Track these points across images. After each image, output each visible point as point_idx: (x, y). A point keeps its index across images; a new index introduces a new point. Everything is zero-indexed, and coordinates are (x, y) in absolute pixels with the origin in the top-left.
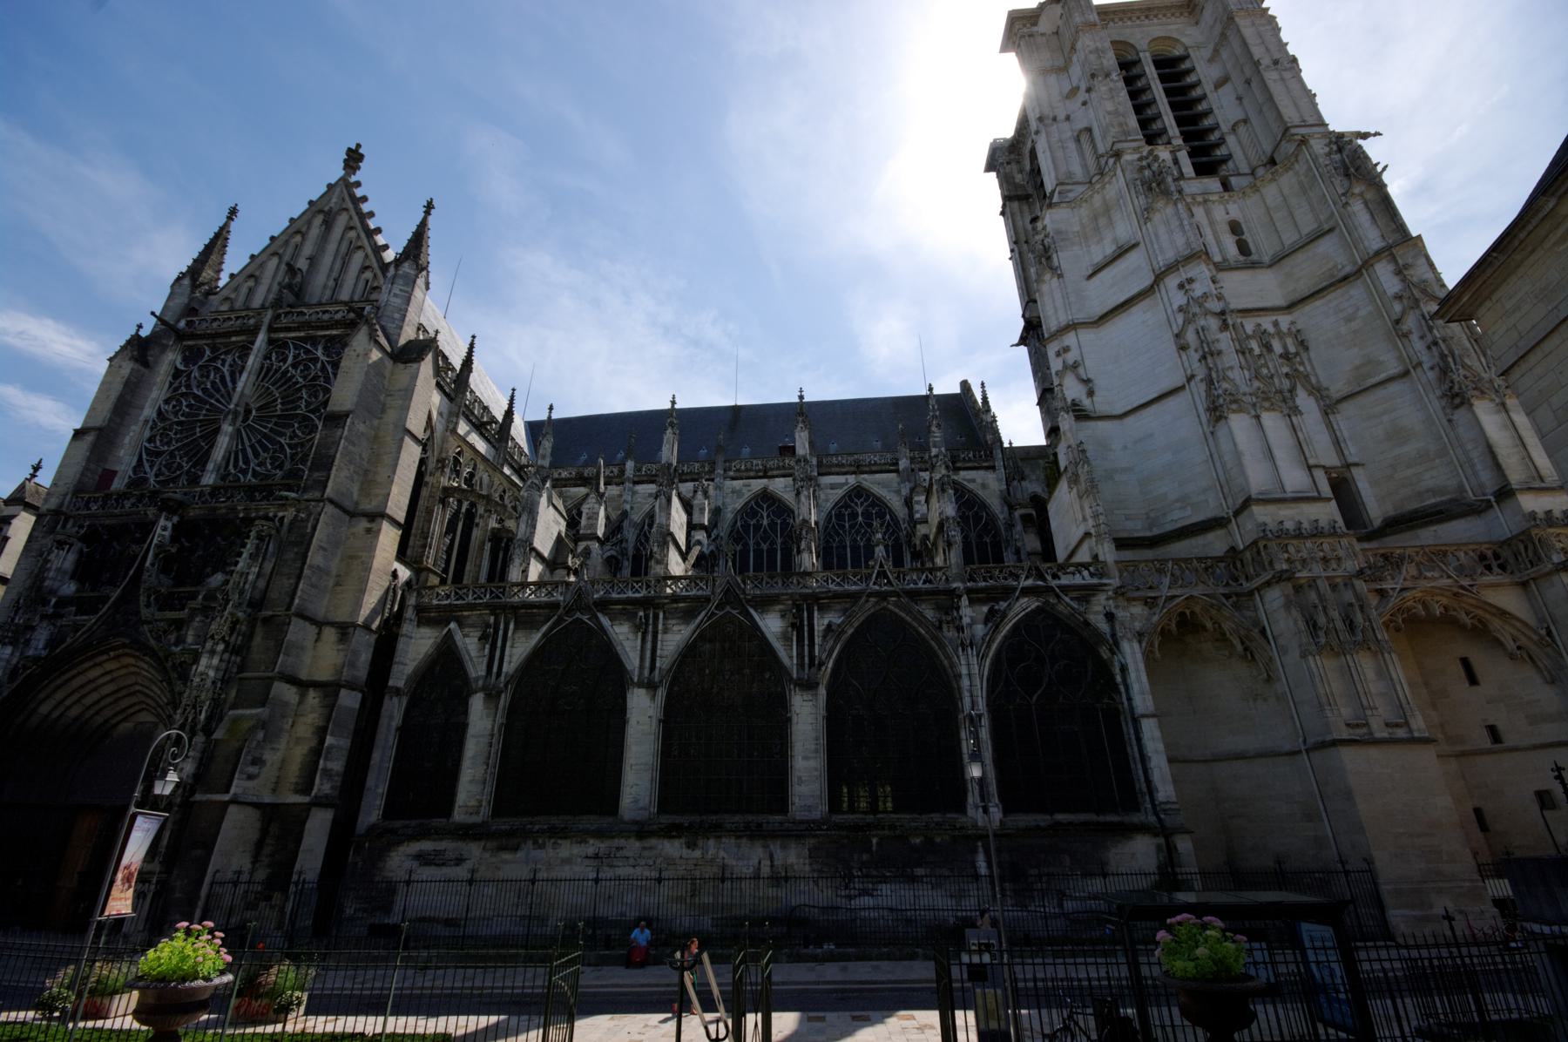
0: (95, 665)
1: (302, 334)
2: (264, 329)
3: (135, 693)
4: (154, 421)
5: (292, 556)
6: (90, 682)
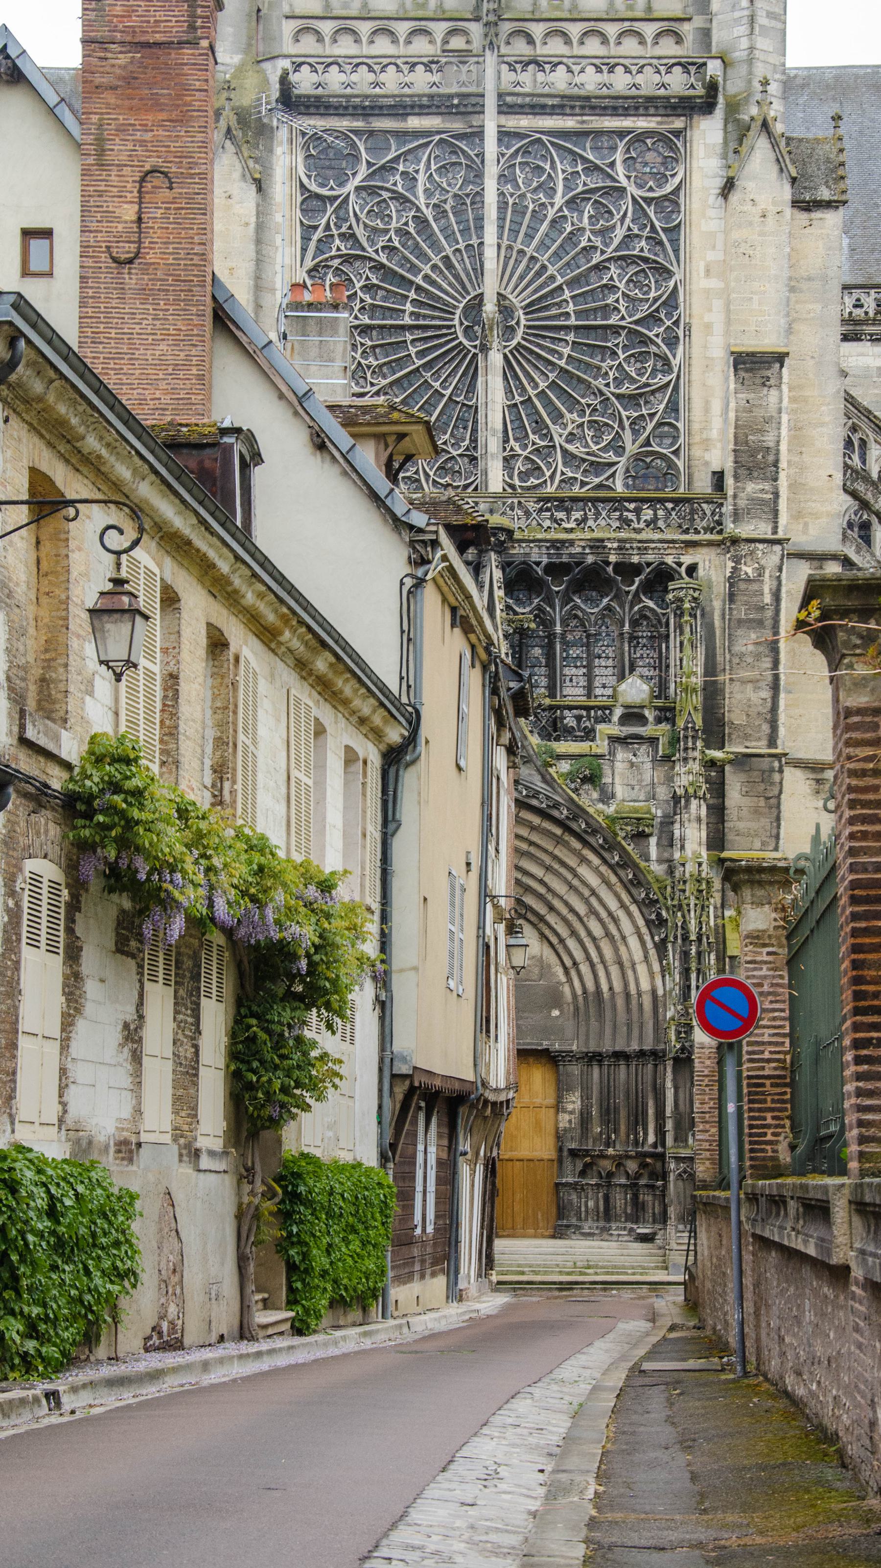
1: (570, 123)
2: (491, 103)
5: (751, 648)
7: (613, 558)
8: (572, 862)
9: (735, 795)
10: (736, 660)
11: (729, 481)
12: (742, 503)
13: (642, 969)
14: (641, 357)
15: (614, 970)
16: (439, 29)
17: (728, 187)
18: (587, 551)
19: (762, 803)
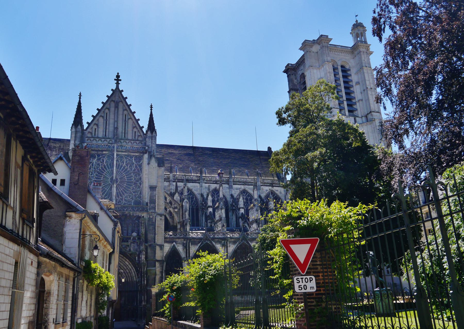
1: (126, 154)
8: (124, 261)
9: (149, 250)
11: (149, 204)
12: (151, 207)
13: (135, 278)
14: (136, 186)
15: (130, 278)
16: (108, 140)
17: (149, 164)
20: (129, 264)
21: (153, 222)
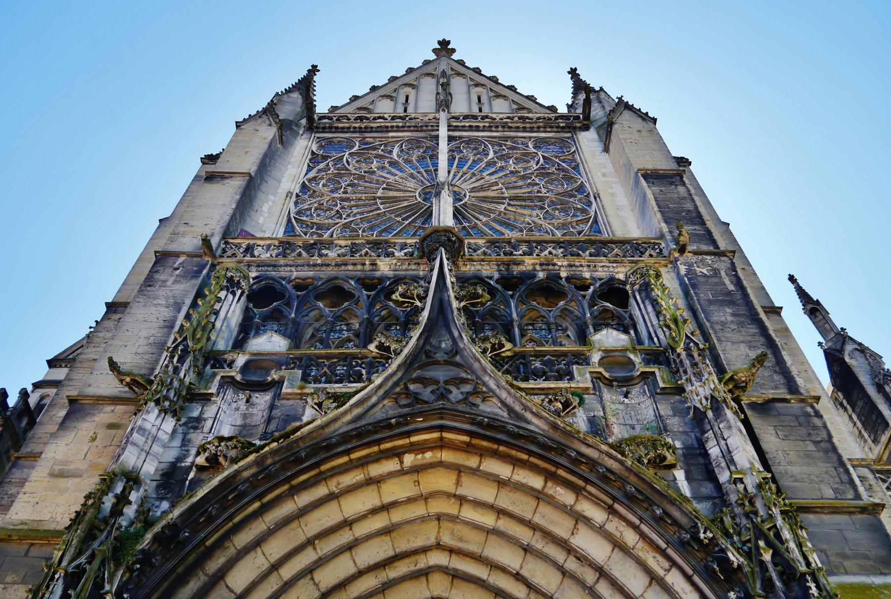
0: (371, 482)
3: (425, 573)
4: (297, 196)
5: (730, 318)
6: (347, 524)
7: (563, 274)
10: (718, 327)
18: (538, 267)
19: (811, 447)
20: (618, 545)
21: (729, 293)
